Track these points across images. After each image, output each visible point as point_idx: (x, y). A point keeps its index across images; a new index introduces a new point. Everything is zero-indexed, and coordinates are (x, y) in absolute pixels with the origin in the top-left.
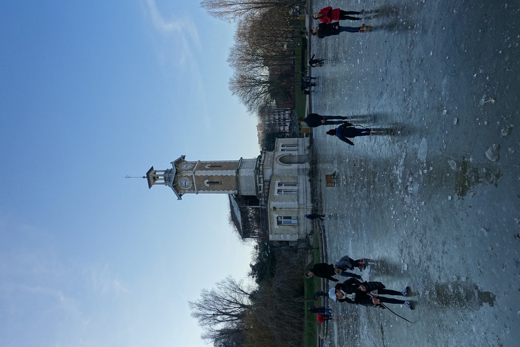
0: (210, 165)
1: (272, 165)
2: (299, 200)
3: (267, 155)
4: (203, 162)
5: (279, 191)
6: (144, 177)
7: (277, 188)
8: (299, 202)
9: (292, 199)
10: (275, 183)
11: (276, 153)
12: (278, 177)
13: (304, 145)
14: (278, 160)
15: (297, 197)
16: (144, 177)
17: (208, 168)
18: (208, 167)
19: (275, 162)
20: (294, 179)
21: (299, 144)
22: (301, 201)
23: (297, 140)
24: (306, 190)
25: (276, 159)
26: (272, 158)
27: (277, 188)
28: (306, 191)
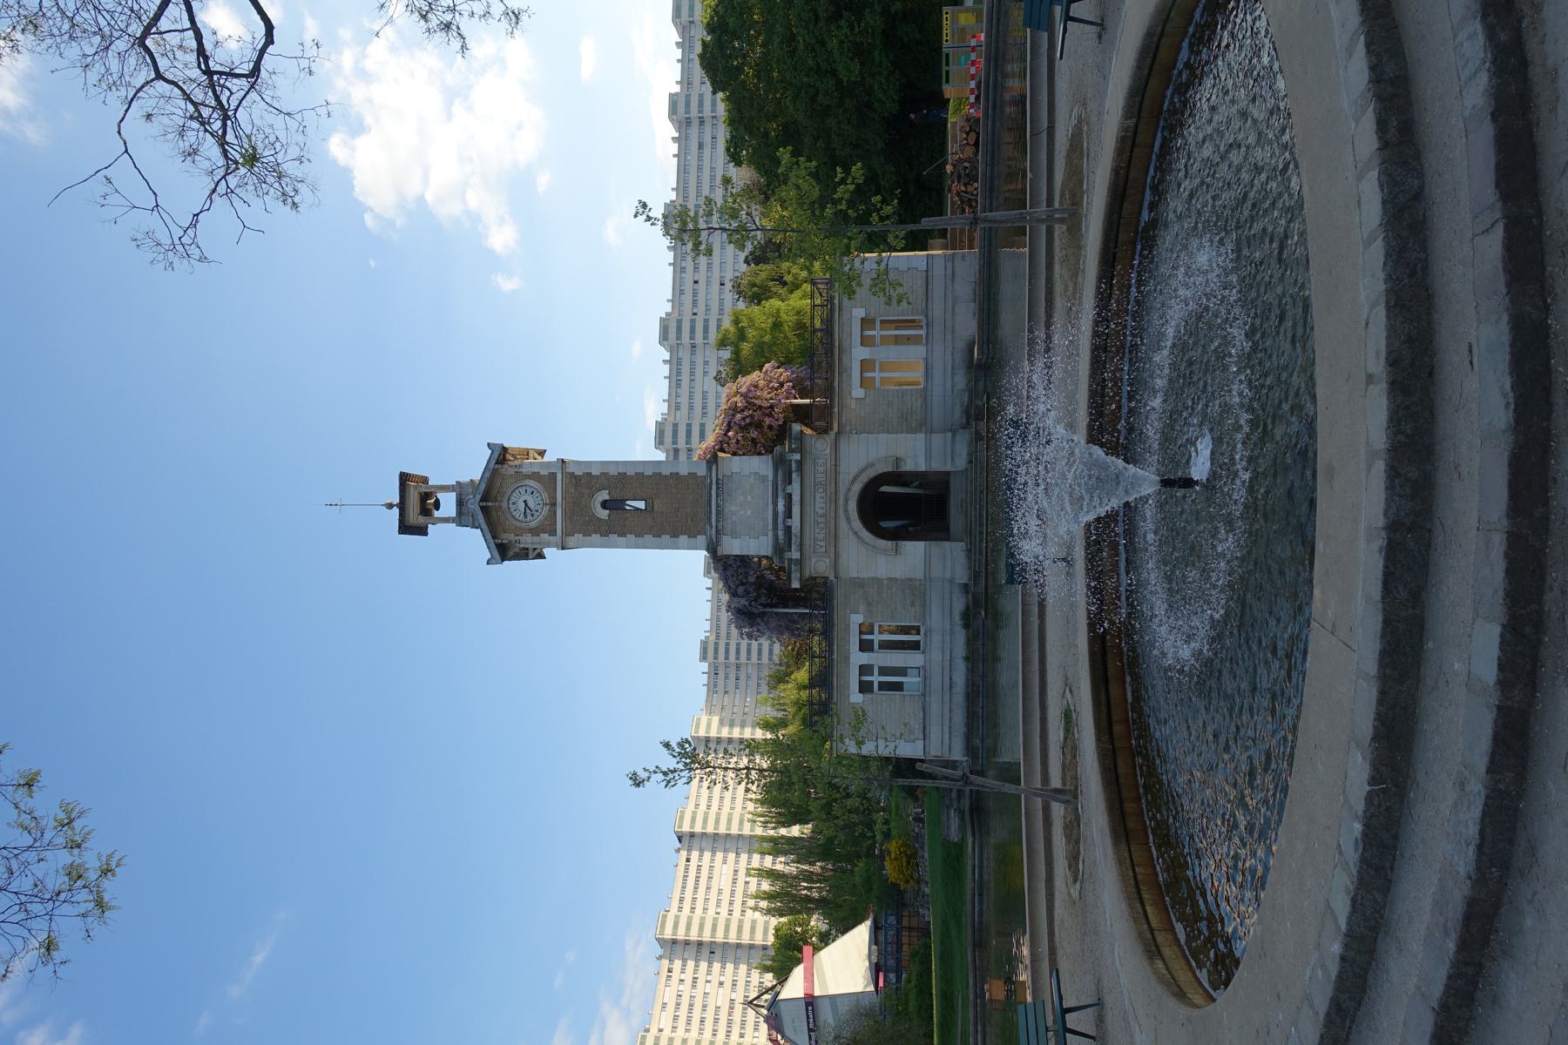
0: (604, 495)
1: (832, 555)
2: (927, 732)
3: (808, 466)
4: (578, 472)
6: (390, 506)
7: (858, 658)
8: (927, 740)
10: (847, 630)
11: (843, 445)
12: (859, 583)
13: (953, 337)
14: (853, 506)
15: (921, 714)
16: (390, 506)
17: (604, 514)
18: (604, 505)
19: (843, 524)
20: (913, 604)
21: (930, 314)
23: (924, 274)
24: (950, 679)
25: (847, 500)
26: (828, 492)
27: (858, 658)
28: (951, 687)
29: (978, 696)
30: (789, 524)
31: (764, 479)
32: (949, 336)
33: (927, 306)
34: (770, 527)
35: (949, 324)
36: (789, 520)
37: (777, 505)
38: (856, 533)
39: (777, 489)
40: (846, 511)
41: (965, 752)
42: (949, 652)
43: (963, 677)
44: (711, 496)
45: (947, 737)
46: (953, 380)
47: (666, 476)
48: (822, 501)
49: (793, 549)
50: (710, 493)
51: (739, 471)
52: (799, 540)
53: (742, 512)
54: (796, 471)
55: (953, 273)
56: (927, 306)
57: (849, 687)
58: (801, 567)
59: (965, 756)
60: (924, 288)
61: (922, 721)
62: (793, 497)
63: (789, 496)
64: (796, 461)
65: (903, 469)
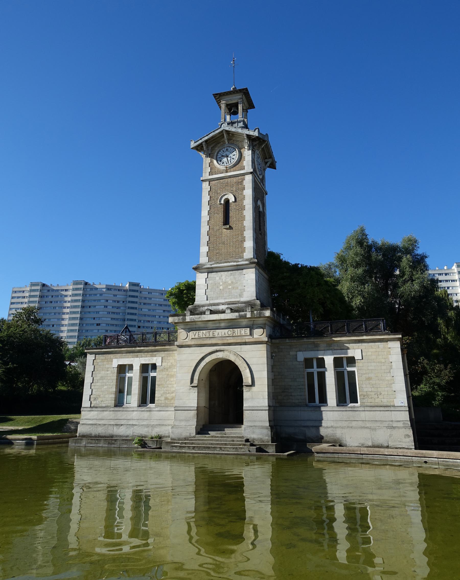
2: (94, 409)
5: (131, 367)
9: (99, 396)
14: (220, 355)
15: (104, 405)
22: (94, 414)
23: (392, 404)
24: (122, 425)
29: (109, 443)
30: (206, 313)
31: (241, 296)
32: (345, 424)
33: (367, 406)
34: (212, 302)
35: (354, 424)
36: (209, 313)
37: (223, 305)
38: (203, 359)
39: (232, 304)
40: (217, 351)
41: (81, 435)
42: (137, 423)
43: (121, 434)
44: (229, 262)
45: (91, 422)
46: (312, 426)
47: (243, 234)
48: (223, 334)
49: (191, 316)
50: (232, 262)
51: (246, 279)
52: (197, 320)
53: (221, 283)
54: (239, 315)
55: (394, 428)
56: (367, 406)
57: (122, 358)
58: (181, 323)
59: (79, 434)
60: (382, 404)
61: (100, 405)
62: (223, 314)
63: (223, 312)
64: (246, 315)
65: (245, 389)
